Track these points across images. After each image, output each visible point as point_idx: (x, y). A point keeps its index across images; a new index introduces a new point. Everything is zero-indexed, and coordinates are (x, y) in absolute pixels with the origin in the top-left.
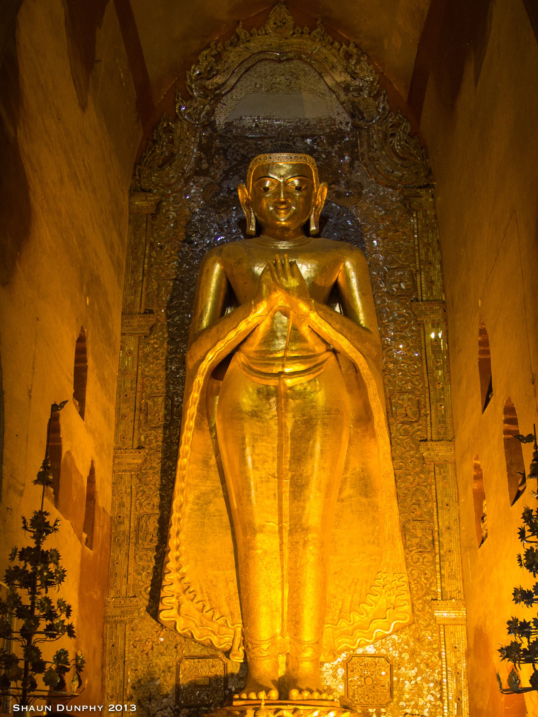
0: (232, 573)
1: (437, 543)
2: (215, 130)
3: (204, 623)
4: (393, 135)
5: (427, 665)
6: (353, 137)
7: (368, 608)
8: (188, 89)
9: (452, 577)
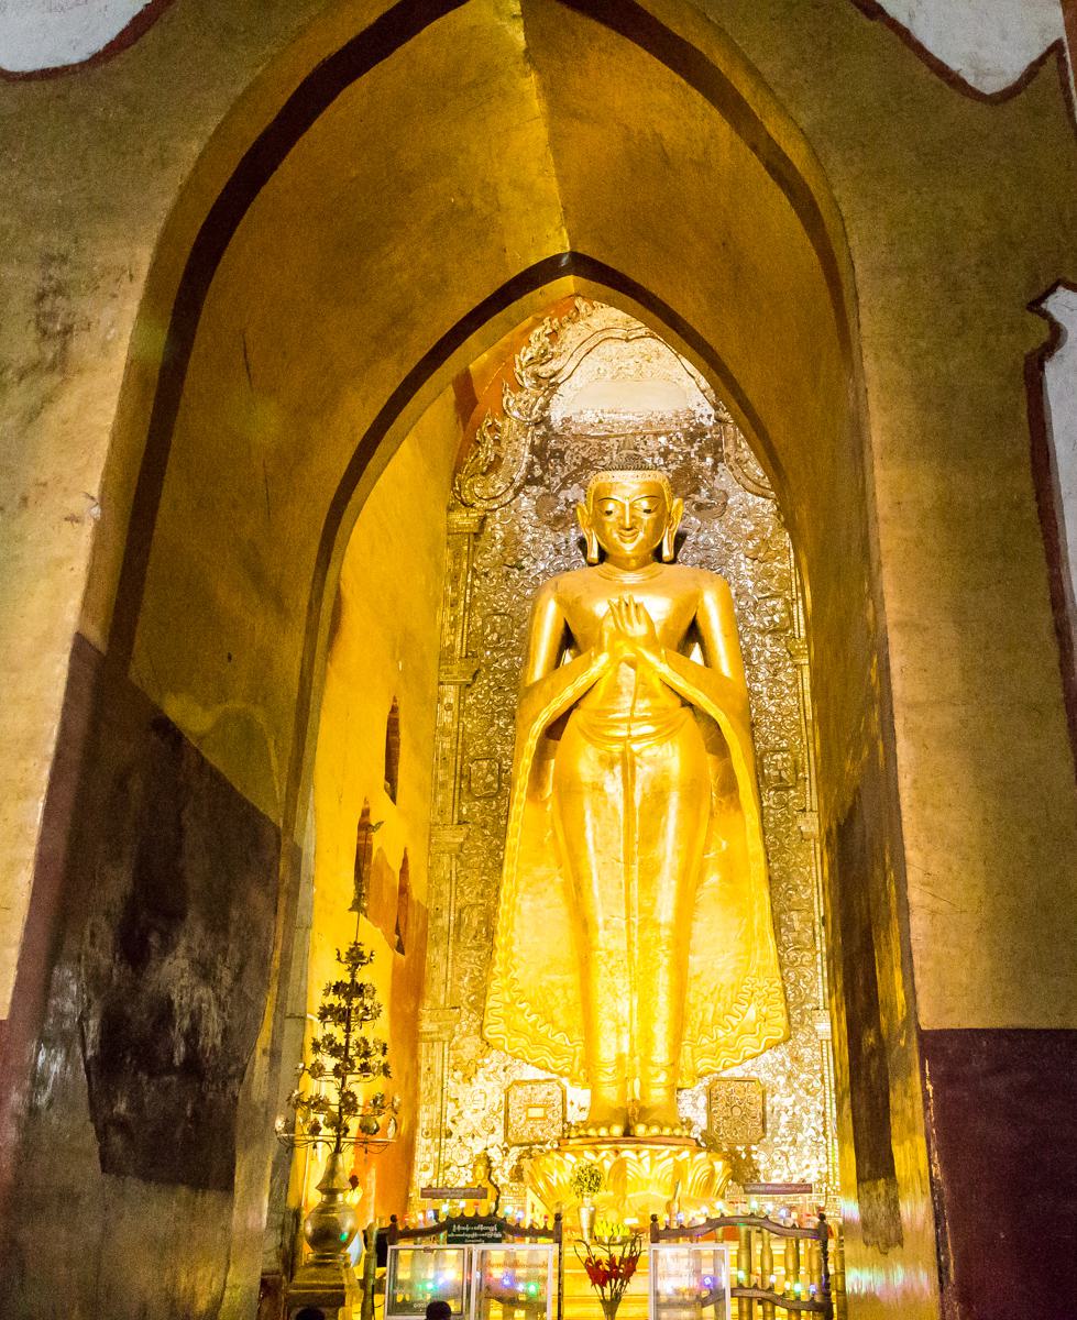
0: (572, 979)
2: (550, 428)
7: (734, 1021)
8: (518, 377)
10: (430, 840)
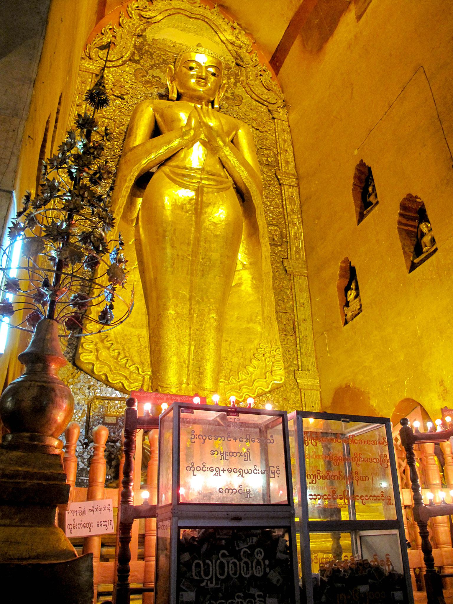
1: (297, 329)
2: (145, 41)
3: (118, 368)
4: (261, 75)
6: (236, 70)
8: (129, 13)
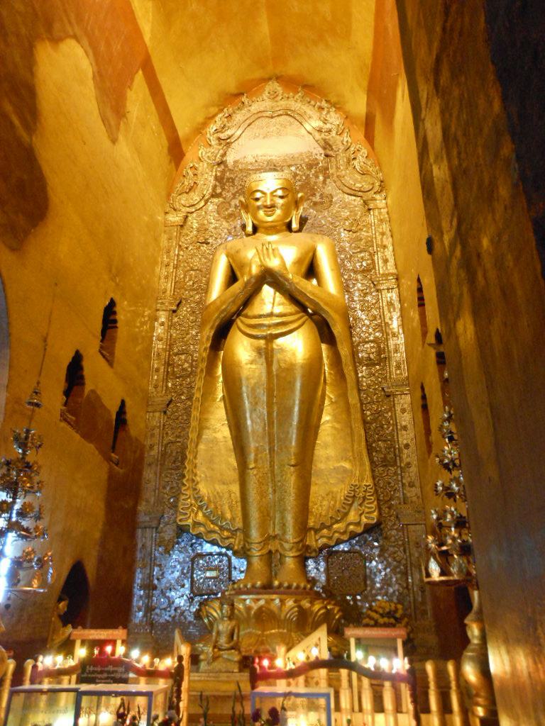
1: (398, 458)
2: (226, 166)
4: (354, 159)
5: (394, 559)
9: (411, 485)
10: (148, 403)
